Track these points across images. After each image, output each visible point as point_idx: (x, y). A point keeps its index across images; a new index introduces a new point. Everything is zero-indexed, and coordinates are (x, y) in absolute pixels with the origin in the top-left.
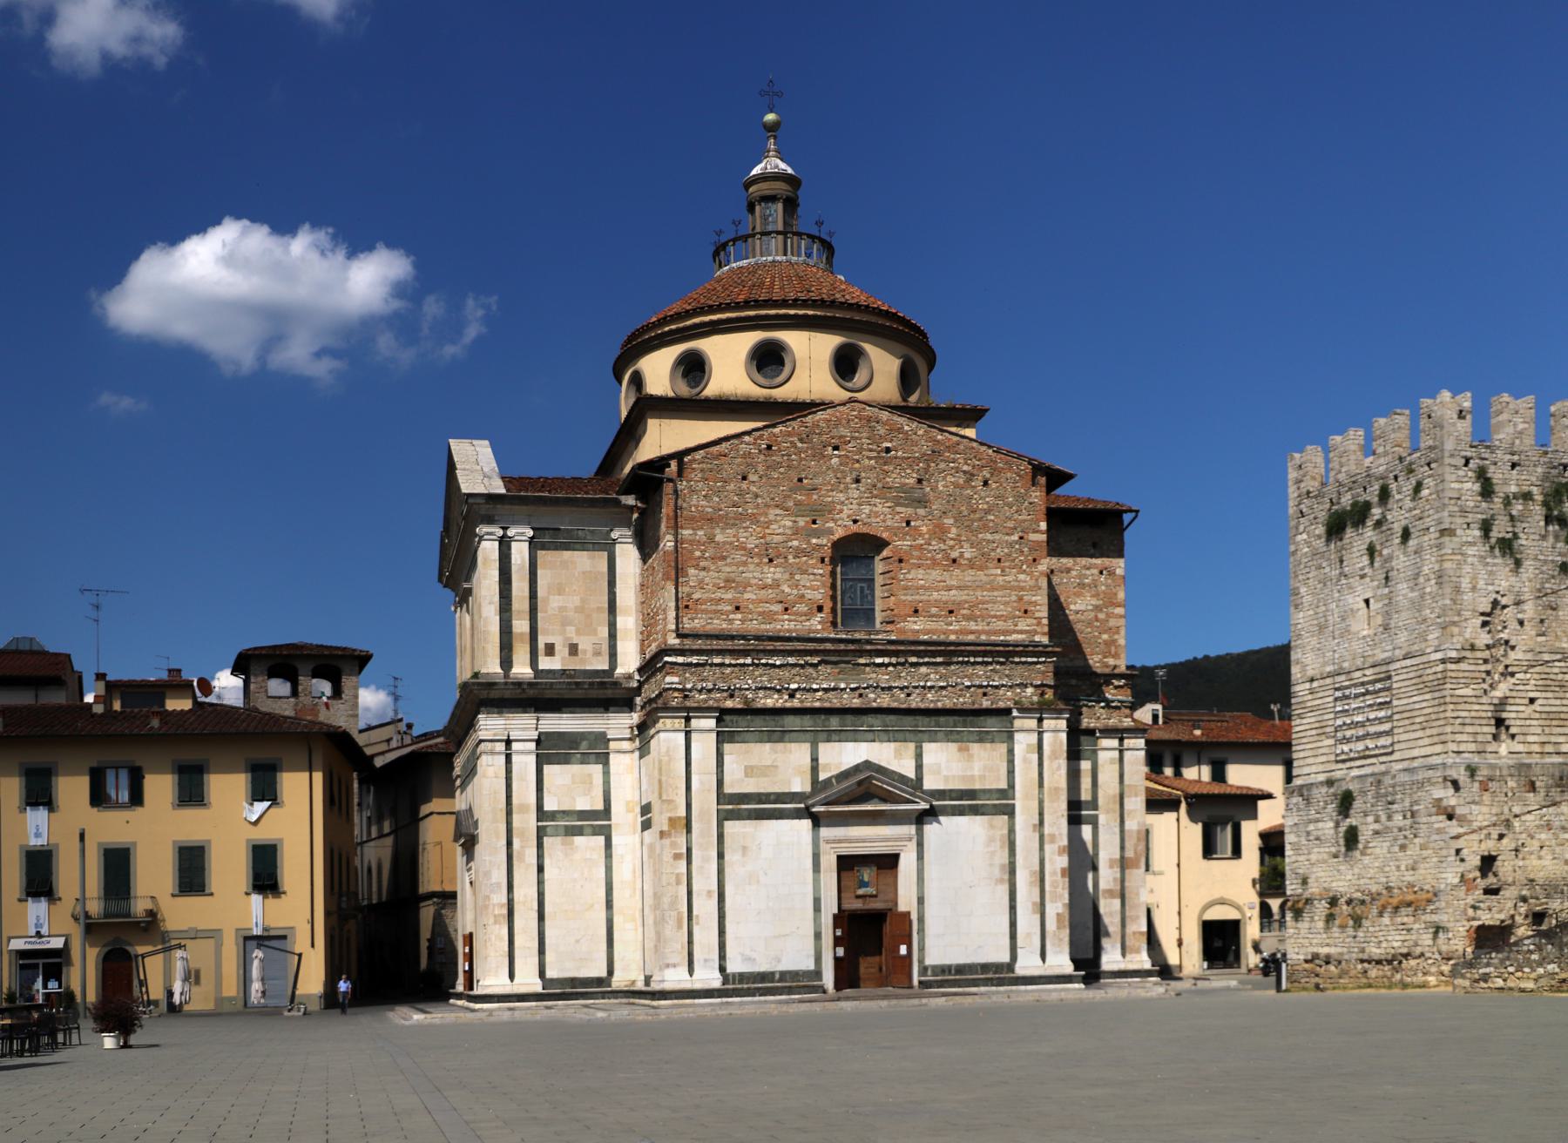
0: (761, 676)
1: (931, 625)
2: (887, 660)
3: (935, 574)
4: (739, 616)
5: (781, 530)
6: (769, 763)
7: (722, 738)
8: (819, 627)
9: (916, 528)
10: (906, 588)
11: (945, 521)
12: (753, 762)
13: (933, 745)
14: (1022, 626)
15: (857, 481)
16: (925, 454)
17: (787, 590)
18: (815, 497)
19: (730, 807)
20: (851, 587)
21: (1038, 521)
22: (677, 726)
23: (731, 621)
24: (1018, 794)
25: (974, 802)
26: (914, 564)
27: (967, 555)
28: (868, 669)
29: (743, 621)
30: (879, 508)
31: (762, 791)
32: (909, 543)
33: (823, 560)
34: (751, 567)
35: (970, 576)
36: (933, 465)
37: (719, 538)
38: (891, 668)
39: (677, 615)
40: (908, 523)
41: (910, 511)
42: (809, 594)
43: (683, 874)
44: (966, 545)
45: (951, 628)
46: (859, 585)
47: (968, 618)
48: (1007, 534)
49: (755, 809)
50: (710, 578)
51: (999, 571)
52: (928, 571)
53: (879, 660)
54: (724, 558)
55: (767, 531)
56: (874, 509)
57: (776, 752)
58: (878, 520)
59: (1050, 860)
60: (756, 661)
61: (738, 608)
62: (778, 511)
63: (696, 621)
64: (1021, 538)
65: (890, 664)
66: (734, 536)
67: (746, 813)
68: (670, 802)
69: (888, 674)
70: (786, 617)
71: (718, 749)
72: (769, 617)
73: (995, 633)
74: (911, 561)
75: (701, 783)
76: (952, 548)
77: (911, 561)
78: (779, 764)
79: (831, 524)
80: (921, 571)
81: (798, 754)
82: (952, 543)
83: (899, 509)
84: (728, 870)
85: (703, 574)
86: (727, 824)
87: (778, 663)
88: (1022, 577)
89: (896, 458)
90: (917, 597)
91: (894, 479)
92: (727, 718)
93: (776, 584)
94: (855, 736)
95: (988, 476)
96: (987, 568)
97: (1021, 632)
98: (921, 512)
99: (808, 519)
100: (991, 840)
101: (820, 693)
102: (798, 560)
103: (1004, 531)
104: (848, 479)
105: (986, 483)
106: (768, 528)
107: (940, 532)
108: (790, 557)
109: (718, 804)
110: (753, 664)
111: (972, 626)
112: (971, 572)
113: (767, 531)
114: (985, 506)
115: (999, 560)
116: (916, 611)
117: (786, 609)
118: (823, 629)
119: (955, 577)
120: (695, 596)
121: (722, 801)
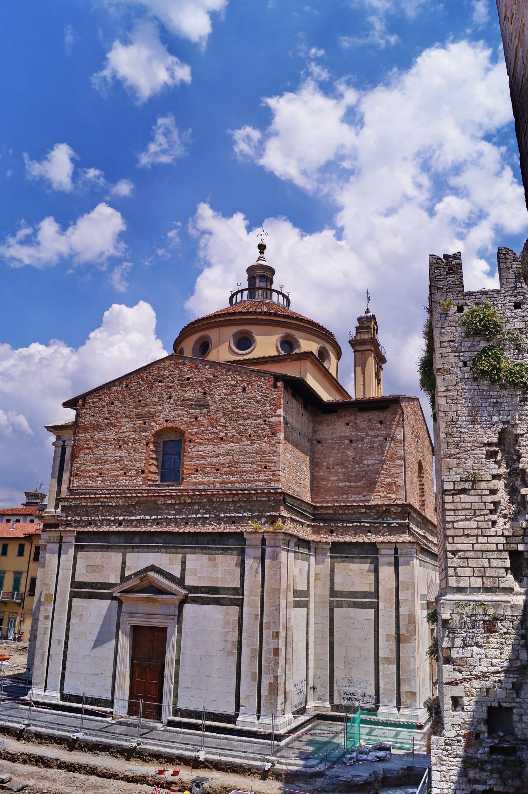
0: (105, 513)
1: (206, 479)
2: (173, 502)
3: (210, 448)
4: (101, 479)
5: (127, 430)
6: (99, 564)
7: (78, 548)
8: (141, 483)
9: (200, 421)
10: (192, 457)
11: (218, 415)
12: (91, 563)
13: (193, 556)
14: (262, 476)
15: (170, 398)
16: (208, 379)
17: (127, 463)
18: (146, 409)
19: (77, 590)
20: (169, 458)
21: (275, 410)
22: (56, 540)
23: (96, 481)
24: (245, 592)
25: (217, 596)
26: (197, 442)
27: (229, 435)
28: (163, 507)
29: (102, 481)
30: (180, 412)
31: (94, 581)
32: (196, 430)
33: (147, 444)
34: (110, 451)
35: (230, 447)
36: (214, 383)
37: (97, 436)
38: (177, 507)
39: (70, 479)
40: (196, 418)
41: (198, 411)
42: (138, 464)
43: (47, 628)
44: (230, 428)
45: (217, 480)
46: (173, 457)
47: (226, 473)
48: (256, 420)
49: (89, 592)
50: (90, 458)
51: (249, 443)
52: (205, 446)
53: (169, 502)
54: (98, 447)
55: (121, 431)
56: (177, 413)
57: (104, 558)
58: (179, 418)
59: (267, 641)
60: (103, 504)
61: (101, 474)
62: (127, 420)
63: (80, 482)
64: (265, 421)
65: (175, 504)
66: (104, 435)
67: (84, 594)
68: (47, 584)
69: (174, 510)
70: (125, 478)
71: (75, 555)
72: (115, 478)
73: (244, 482)
74: (197, 441)
75: (63, 575)
76: (221, 431)
77: (197, 441)
78: (104, 565)
79: (153, 424)
80: (202, 446)
81: (116, 558)
82: (221, 428)
83: (191, 411)
84: (71, 628)
85: (87, 456)
86: (74, 599)
87: (114, 504)
88: (264, 445)
89: (192, 383)
90: (198, 462)
91: (190, 394)
92: (82, 537)
93: (121, 459)
94: (149, 549)
95: (246, 385)
96: (242, 441)
97: (261, 481)
98: (205, 411)
99: (141, 422)
100: (227, 623)
101: (135, 523)
102: (134, 445)
103: (254, 418)
104: (165, 397)
105: (244, 390)
106: (121, 429)
107: (214, 422)
108: (130, 444)
109: (71, 587)
110: (101, 506)
111: (231, 478)
112: (232, 444)
113: (121, 431)
114: (243, 404)
115: (250, 436)
116: (197, 471)
117: (125, 473)
118: (143, 484)
119: (223, 448)
120: (82, 469)
121: (73, 585)
